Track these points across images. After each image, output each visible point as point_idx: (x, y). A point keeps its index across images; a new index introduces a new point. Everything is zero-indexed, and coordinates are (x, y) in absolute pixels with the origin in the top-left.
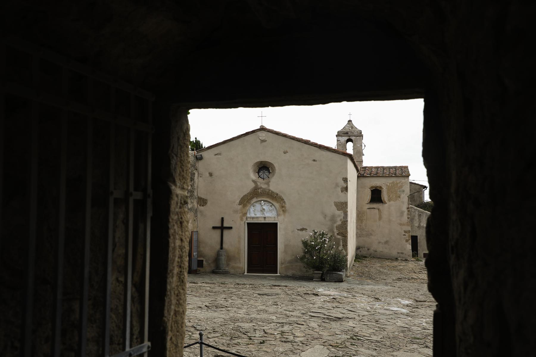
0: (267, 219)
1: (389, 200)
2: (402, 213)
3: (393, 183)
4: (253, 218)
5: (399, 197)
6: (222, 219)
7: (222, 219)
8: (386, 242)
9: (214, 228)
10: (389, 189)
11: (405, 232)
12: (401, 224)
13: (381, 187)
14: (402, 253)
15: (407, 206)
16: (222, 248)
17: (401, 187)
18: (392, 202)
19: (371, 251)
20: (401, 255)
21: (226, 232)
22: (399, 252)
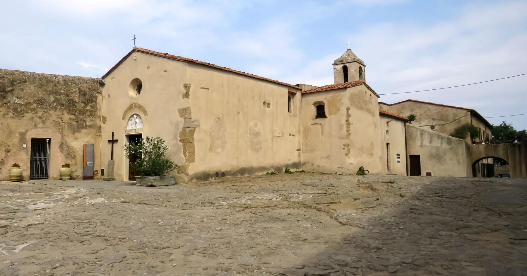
0: (137, 131)
1: (330, 115)
2: (341, 127)
3: (332, 97)
4: (129, 131)
5: (339, 110)
6: (113, 133)
7: (113, 133)
8: (328, 157)
9: (109, 141)
10: (329, 102)
11: (345, 145)
12: (341, 138)
13: (323, 102)
14: (342, 168)
15: (346, 119)
16: (112, 159)
17: (340, 99)
18: (332, 116)
19: (315, 166)
20: (341, 169)
21: (115, 145)
22: (339, 166)
